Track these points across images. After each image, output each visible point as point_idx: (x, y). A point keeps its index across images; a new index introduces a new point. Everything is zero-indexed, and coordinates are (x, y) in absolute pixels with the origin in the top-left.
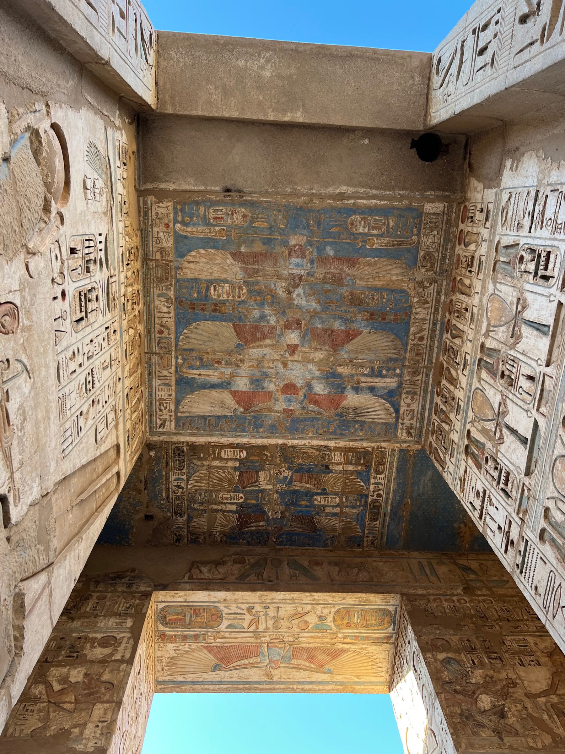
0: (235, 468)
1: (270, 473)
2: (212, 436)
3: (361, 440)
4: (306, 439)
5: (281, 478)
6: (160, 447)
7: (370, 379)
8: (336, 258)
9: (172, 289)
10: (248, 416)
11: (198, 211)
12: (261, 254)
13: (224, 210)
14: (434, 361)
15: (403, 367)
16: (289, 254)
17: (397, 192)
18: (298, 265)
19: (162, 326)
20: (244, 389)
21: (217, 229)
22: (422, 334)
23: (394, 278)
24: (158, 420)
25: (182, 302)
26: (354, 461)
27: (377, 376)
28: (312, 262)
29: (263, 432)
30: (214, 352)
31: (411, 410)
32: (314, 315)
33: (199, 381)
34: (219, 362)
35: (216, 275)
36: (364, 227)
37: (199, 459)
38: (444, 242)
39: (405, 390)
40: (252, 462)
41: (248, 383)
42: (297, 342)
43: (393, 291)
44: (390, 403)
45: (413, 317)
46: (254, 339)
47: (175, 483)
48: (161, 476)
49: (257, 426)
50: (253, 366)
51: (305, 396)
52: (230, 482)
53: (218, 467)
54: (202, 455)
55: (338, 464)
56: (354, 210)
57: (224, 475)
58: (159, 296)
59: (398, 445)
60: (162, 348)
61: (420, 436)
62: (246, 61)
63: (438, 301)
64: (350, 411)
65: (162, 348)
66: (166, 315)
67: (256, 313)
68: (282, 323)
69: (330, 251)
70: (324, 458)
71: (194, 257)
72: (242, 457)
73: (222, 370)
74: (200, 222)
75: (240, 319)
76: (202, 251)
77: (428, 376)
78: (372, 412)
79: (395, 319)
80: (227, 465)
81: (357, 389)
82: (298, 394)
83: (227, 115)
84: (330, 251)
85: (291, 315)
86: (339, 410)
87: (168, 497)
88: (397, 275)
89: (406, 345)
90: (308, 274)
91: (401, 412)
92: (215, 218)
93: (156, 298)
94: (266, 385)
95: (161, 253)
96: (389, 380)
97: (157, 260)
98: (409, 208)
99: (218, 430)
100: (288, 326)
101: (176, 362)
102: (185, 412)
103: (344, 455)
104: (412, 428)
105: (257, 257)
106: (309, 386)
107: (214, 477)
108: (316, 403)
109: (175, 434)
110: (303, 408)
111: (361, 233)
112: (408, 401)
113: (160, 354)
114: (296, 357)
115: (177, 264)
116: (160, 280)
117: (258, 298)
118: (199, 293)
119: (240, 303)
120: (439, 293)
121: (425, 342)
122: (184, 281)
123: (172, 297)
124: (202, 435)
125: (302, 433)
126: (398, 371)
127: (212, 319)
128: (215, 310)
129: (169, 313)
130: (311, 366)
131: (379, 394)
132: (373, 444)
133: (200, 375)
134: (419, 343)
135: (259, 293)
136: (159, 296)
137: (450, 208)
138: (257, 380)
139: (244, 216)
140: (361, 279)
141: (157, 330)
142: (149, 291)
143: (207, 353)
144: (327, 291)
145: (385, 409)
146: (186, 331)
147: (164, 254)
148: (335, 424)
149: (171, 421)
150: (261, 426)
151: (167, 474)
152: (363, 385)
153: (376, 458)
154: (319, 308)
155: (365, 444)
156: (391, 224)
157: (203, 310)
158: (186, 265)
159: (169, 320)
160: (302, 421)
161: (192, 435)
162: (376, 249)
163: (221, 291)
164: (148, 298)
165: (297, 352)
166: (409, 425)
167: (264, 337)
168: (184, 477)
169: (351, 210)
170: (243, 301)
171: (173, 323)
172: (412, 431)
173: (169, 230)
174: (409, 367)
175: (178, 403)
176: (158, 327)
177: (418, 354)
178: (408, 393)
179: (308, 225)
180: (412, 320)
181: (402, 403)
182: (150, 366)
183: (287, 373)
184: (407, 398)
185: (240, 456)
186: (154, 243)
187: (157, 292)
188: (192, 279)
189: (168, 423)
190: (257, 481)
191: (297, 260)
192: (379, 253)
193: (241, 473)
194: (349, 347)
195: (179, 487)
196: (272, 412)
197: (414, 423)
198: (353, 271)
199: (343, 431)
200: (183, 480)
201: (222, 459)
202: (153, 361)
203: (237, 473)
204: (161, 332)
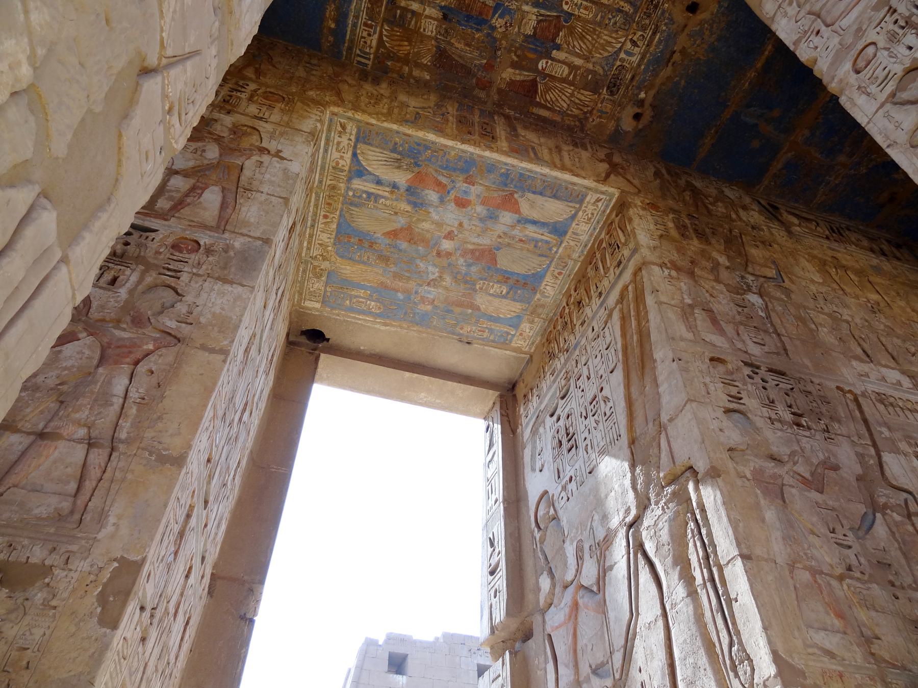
0: (558, 48)
1: (519, 28)
2: (556, 178)
3: (398, 132)
4: (459, 149)
5: (507, 18)
6: (630, 100)
7: (380, 193)
8: (397, 291)
10: (511, 188)
12: (456, 305)
14: (314, 194)
15: (345, 196)
16: (434, 301)
17: (342, 318)
18: (429, 292)
20: (507, 213)
21: (485, 326)
22: (325, 220)
23: (348, 267)
24: (600, 206)
26: (409, 16)
27: (372, 194)
28: (416, 292)
29: (501, 168)
30: (522, 249)
31: (339, 151)
32: (423, 258)
33: (545, 229)
34: (521, 240)
35: (496, 302)
36: (370, 304)
37: (594, 73)
38: (304, 282)
39: (344, 174)
40: (535, 51)
41: (501, 218)
42: (444, 241)
43: (350, 259)
44: (362, 166)
45: (333, 236)
46: (483, 252)
47: (637, 50)
48: (647, 65)
49: (506, 175)
50: (491, 230)
51: (449, 192)
52: (571, 31)
53: (578, 55)
54: (590, 77)
55: (431, 18)
56: (376, 316)
57: (576, 43)
58: (549, 297)
59: (357, 116)
61: (331, 120)
63: (309, 243)
64: (405, 167)
66: (550, 284)
67: (474, 269)
68: (454, 258)
69: (400, 296)
70: (446, 31)
72: (544, 61)
73: (521, 234)
75: (489, 268)
77: (320, 182)
78: (381, 161)
79: (350, 238)
80: (566, 55)
81: (395, 186)
82: (456, 196)
84: (400, 296)
85: (445, 262)
86: (416, 170)
87: (654, 34)
88: (346, 269)
89: (340, 215)
90: (421, 286)
91: (350, 153)
92: (484, 332)
94: (485, 212)
95: (533, 321)
96: (360, 187)
98: (333, 308)
99: (547, 181)
100: (449, 254)
101: (558, 249)
102: (571, 207)
103: (420, 28)
104: (340, 133)
105: (460, 304)
106: (442, 201)
107: (588, 43)
108: (439, 184)
109: (590, 189)
110: (453, 182)
111: (373, 301)
112: (342, 162)
114: (449, 229)
115: (525, 313)
116: (543, 306)
117: (468, 279)
118: (516, 292)
119: (485, 279)
120: (309, 249)
121: (322, 213)
122: (524, 302)
124: (566, 181)
125: (461, 157)
126: (351, 193)
127: (512, 273)
128: (508, 278)
130: (435, 216)
131: (371, 177)
132: (385, 125)
133: (542, 235)
134: (328, 214)
135: (466, 282)
136: (549, 297)
137: (300, 300)
138: (491, 218)
139: (462, 329)
140: (377, 273)
142: (555, 301)
143: (528, 250)
144: (408, 271)
145: (367, 160)
146: (539, 270)
148: (424, 157)
149: (588, 203)
150: (502, 175)
151: (639, 65)
152: (388, 189)
153: (380, 11)
154: (418, 261)
155: (395, 127)
156: (348, 302)
157: (518, 281)
158: (517, 311)
160: (459, 170)
161: (574, 184)
162: (362, 289)
163: (498, 290)
165: (446, 232)
166: (343, 136)
167: (472, 252)
168: (622, 55)
169: (380, 316)
170: (481, 279)
172: (340, 129)
174: (340, 195)
175: (573, 217)
177: (329, 204)
178: (342, 171)
179: (414, 314)
180: (334, 233)
181: (348, 161)
182: (582, 251)
183: (461, 218)
184: (343, 166)
185: (547, 63)
187: (549, 300)
189: (594, 200)
190: (539, 22)
191: (429, 296)
192: (359, 286)
193: (553, 40)
194: (397, 226)
195: (634, 43)
196: (486, 186)
197: (336, 137)
198: (383, 279)
199: (416, 147)
200: (627, 53)
201: (569, 65)
203: (558, 41)
204: (560, 274)
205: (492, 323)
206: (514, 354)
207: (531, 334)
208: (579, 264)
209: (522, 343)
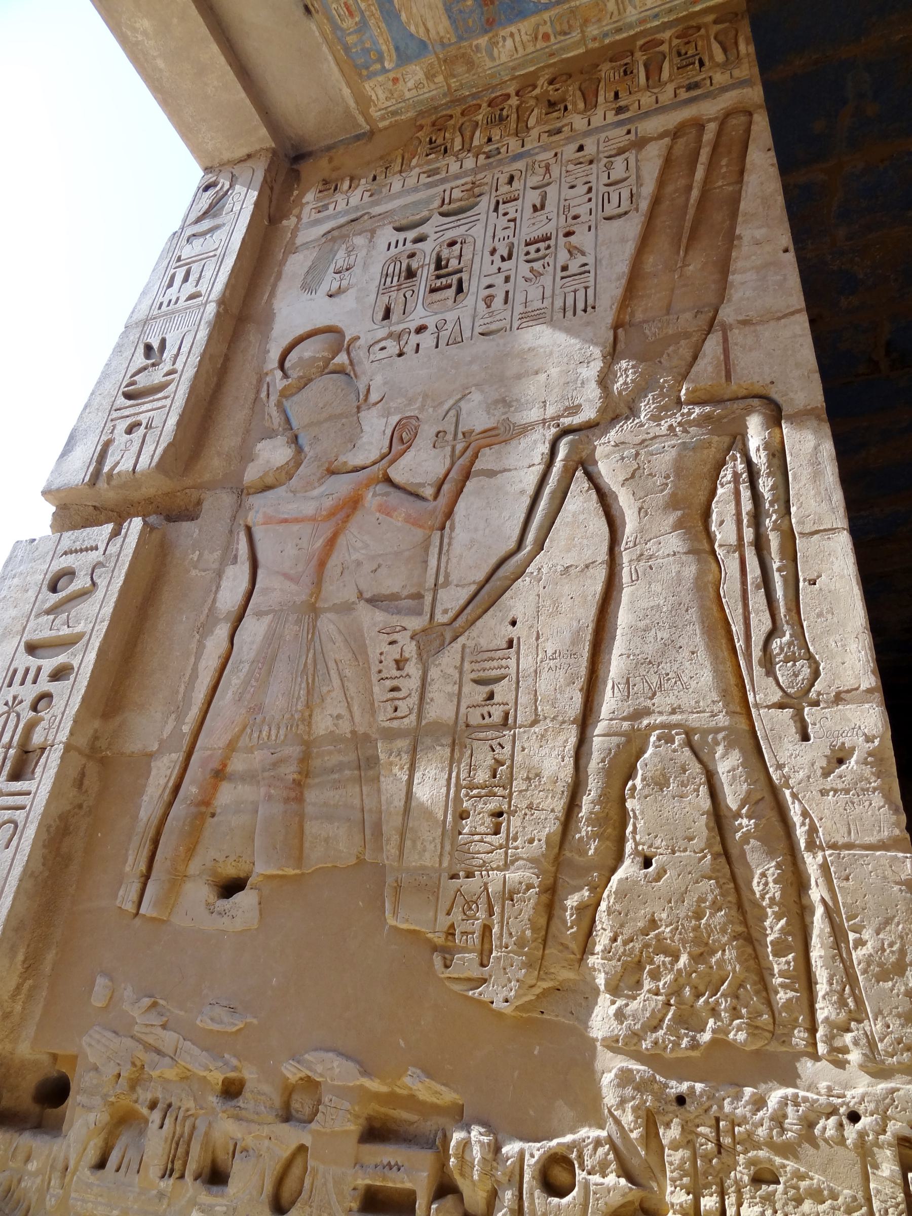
9: (475, 43)
11: (355, 44)
13: (334, 6)
19: (536, 38)
21: (363, 6)
25: (488, 20)
58: (493, 59)
60: (570, 27)
62: (154, 58)
65: (570, 27)
66: (517, 38)
71: (417, 26)
74: (367, 35)
76: (404, 17)
83: (222, 60)
92: (351, 14)
93: (497, 63)
95: (434, 76)
97: (446, 78)
113: (581, 26)
115: (438, 49)
116: (471, 64)
122: (456, 29)
123: (486, 38)
129: (512, 35)
136: (493, 59)
141: (545, 45)
142: (492, 76)
147: (432, 72)
158: (433, 33)
159: (523, 33)
164: (502, 73)
171: (526, 23)
173: (399, 76)
176: (540, 44)
182: (606, 35)
186: (425, 90)
187: (489, 64)
188: (449, 17)
202: (596, 32)
205: (378, 14)
206: (352, 103)
207: (408, 95)
208: (582, 50)
209: (382, 96)
